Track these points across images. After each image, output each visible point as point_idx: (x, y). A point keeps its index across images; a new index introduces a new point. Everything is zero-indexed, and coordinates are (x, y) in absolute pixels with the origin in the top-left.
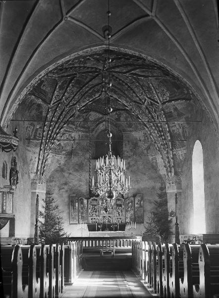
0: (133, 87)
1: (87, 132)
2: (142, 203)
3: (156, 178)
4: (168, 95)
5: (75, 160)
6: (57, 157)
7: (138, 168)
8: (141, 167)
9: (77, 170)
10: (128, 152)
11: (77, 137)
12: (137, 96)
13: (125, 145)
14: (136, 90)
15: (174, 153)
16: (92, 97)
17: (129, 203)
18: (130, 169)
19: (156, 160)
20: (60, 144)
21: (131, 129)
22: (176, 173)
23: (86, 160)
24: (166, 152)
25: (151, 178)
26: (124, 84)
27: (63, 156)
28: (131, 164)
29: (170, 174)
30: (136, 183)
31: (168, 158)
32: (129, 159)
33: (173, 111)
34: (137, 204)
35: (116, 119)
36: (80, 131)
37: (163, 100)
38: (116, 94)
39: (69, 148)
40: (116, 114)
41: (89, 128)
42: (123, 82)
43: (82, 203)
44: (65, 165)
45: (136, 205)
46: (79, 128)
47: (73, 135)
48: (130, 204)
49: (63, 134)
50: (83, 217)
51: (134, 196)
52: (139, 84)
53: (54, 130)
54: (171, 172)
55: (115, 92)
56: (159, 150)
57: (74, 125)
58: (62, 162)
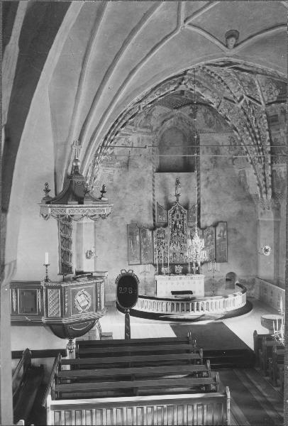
0: (228, 81)
1: (149, 134)
2: (225, 234)
3: (245, 199)
4: (277, 94)
5: (132, 174)
6: (110, 171)
7: (220, 185)
8: (223, 184)
9: (134, 188)
10: (206, 163)
11: (135, 141)
12: (231, 93)
13: (203, 153)
14: (231, 85)
15: (274, 168)
16: (164, 90)
17: (208, 235)
18: (209, 187)
19: (245, 175)
20: (113, 153)
21: (211, 130)
22: (274, 195)
23: (149, 175)
24: (261, 167)
25: (238, 199)
26: (213, 75)
27: (117, 170)
28: (210, 180)
29: (264, 196)
30: (217, 206)
31: (264, 174)
32: (208, 173)
33: (279, 114)
34: (219, 236)
35: (191, 115)
36: (139, 132)
37: (269, 100)
38: (199, 87)
39: (124, 158)
40: (191, 107)
41: (151, 128)
42: (216, 75)
43: (145, 236)
44: (119, 181)
45: (218, 238)
46: (138, 129)
47: (130, 139)
48: (210, 236)
49: (119, 138)
50: (146, 255)
51: (215, 225)
52: (239, 78)
53: (109, 137)
54: (266, 193)
55: (199, 85)
56: (252, 163)
57: (133, 125)
58: (115, 178)
